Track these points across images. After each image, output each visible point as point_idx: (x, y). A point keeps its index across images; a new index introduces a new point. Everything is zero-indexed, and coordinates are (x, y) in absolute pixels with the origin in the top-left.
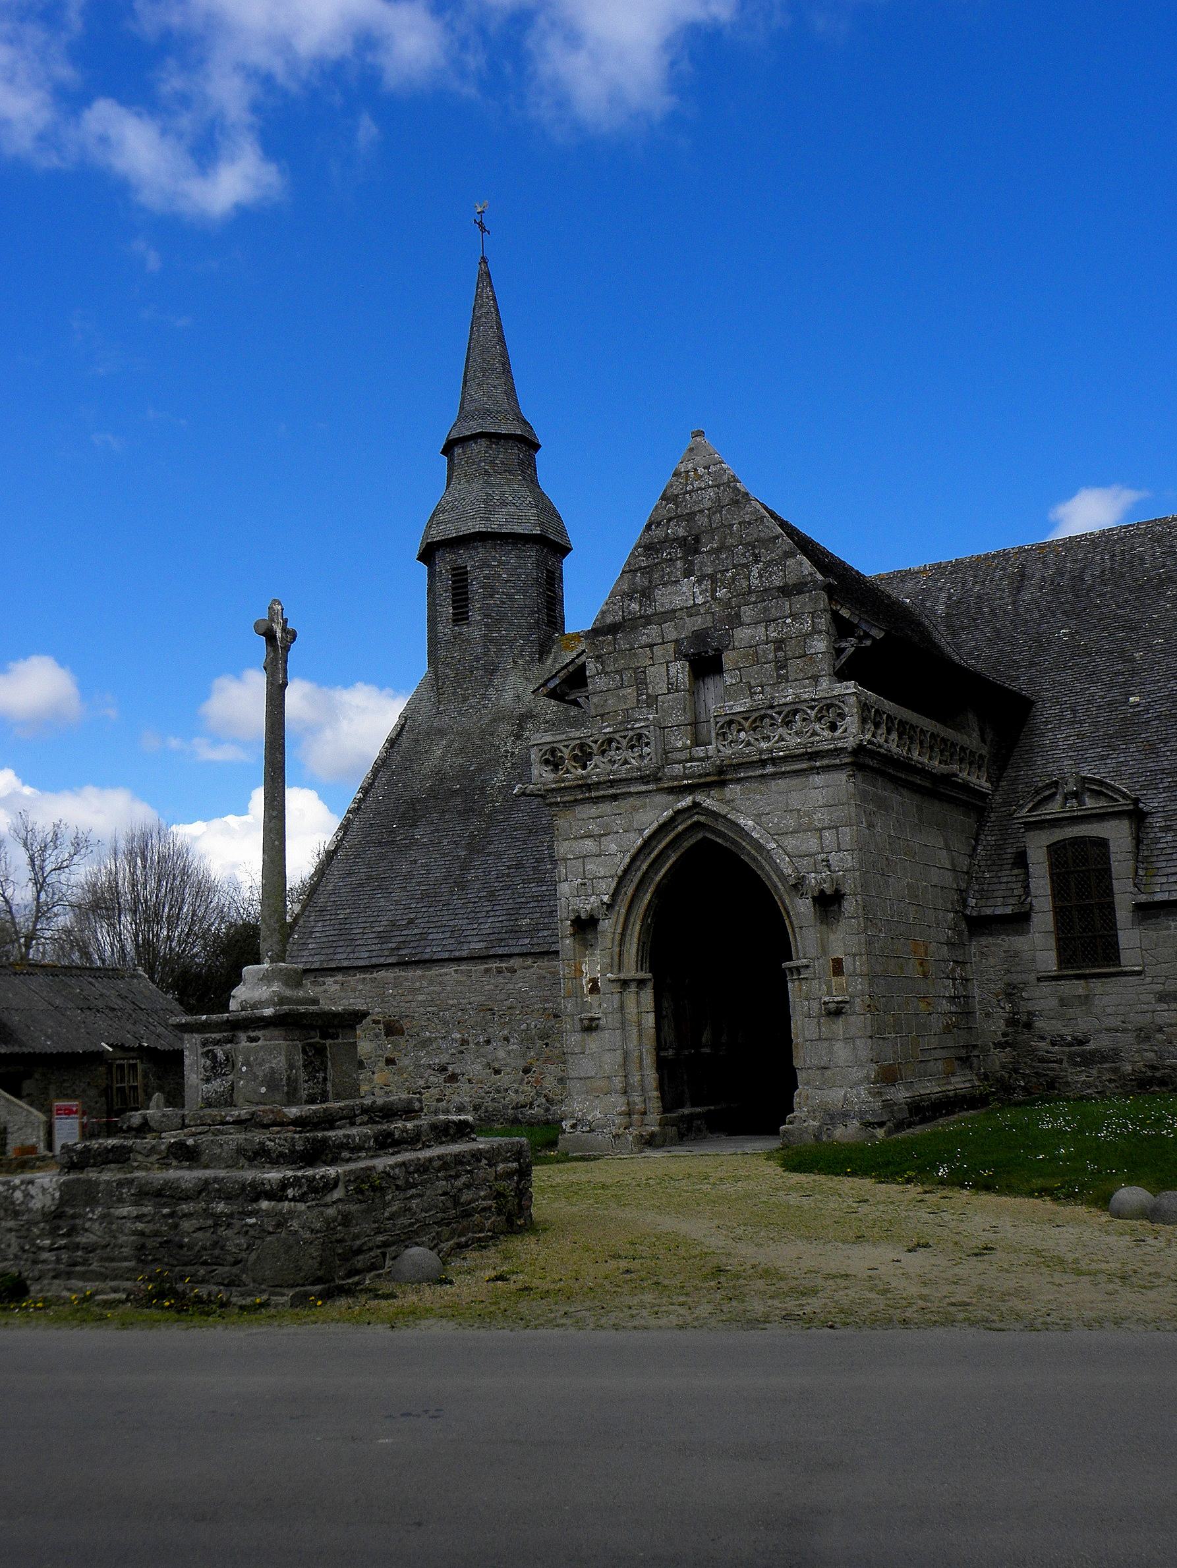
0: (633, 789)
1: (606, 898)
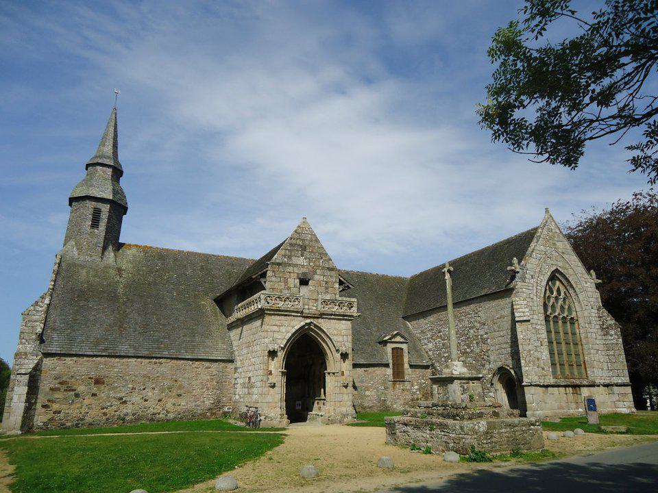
0: (293, 314)
1: (282, 346)
